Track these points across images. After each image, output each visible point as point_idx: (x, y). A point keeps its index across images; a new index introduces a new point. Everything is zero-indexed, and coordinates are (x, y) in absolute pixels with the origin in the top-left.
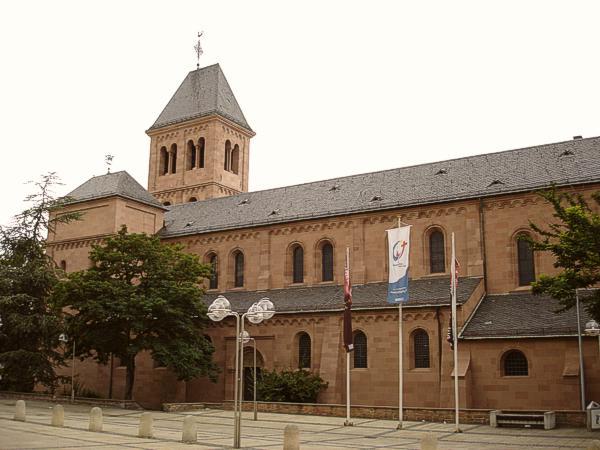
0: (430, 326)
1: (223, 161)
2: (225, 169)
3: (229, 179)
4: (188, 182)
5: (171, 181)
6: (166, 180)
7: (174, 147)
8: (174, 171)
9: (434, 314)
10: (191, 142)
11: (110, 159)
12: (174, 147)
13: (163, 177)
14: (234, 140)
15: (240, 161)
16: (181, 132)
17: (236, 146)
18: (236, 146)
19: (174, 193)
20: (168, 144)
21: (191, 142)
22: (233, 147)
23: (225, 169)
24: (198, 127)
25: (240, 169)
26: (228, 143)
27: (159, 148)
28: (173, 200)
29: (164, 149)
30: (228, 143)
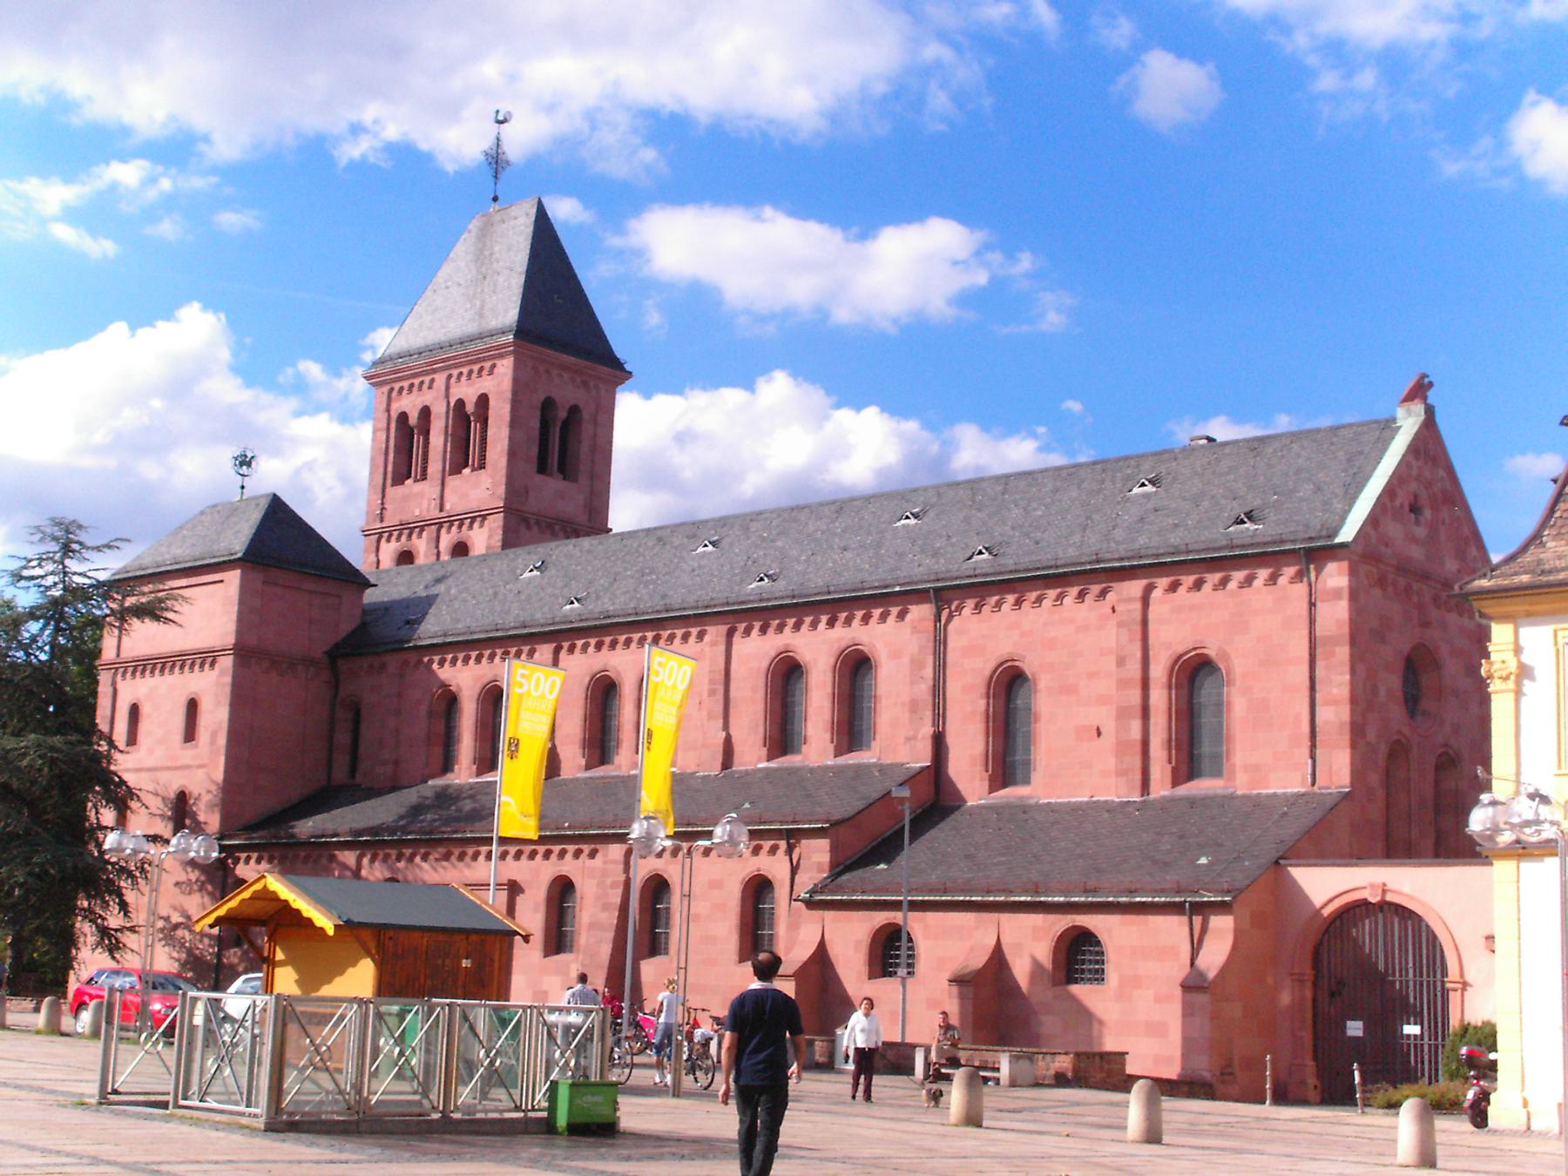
0: (776, 867)
1: (535, 451)
2: (542, 468)
3: (550, 492)
4: (454, 504)
5: (418, 498)
6: (406, 498)
7: (426, 413)
8: (424, 477)
9: (783, 844)
10: (461, 403)
11: (242, 464)
12: (426, 413)
13: (400, 490)
14: (567, 393)
15: (585, 448)
16: (440, 379)
17: (574, 410)
18: (574, 410)
19: (422, 529)
20: (410, 404)
21: (461, 403)
22: (562, 414)
23: (542, 468)
24: (476, 368)
25: (584, 467)
26: (548, 405)
27: (394, 415)
28: (421, 545)
29: (403, 417)
30: (548, 405)
